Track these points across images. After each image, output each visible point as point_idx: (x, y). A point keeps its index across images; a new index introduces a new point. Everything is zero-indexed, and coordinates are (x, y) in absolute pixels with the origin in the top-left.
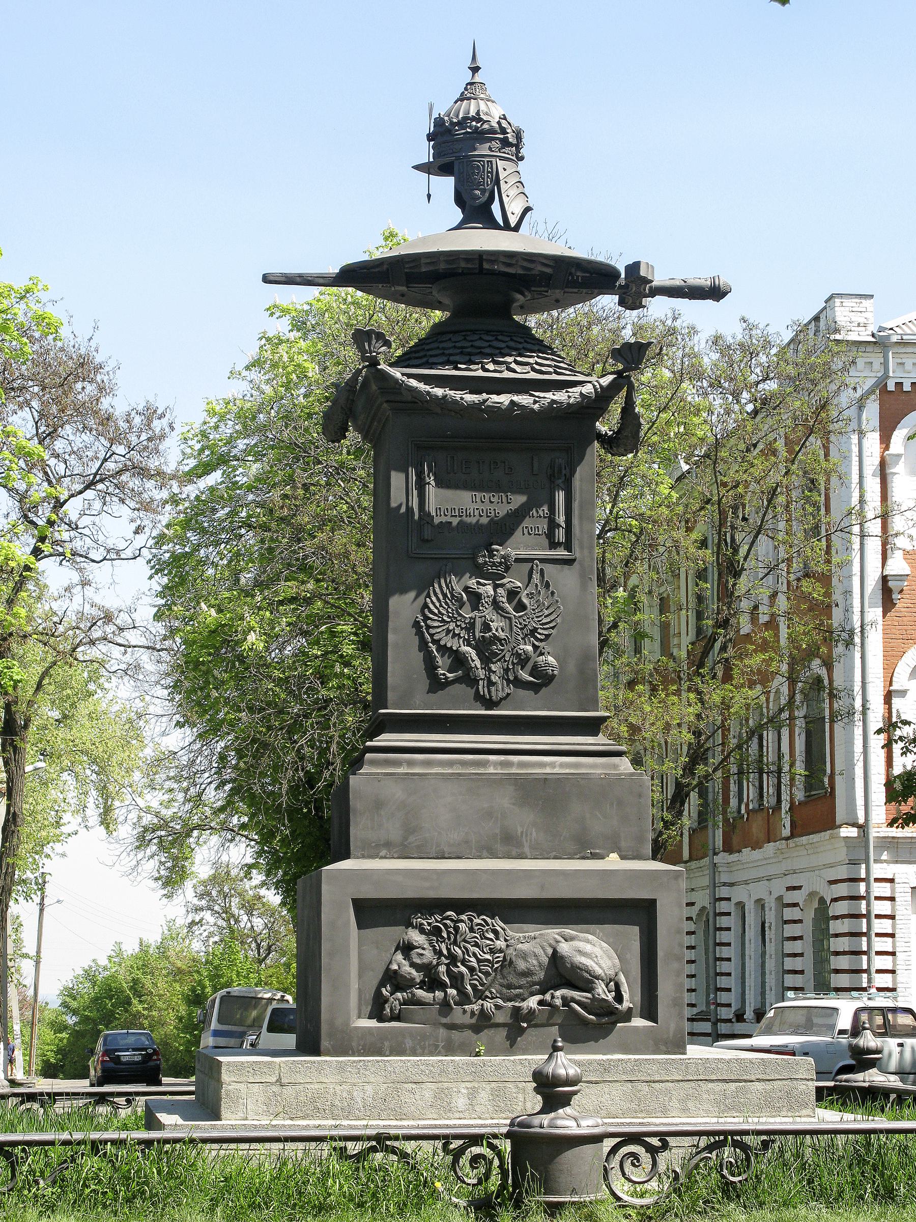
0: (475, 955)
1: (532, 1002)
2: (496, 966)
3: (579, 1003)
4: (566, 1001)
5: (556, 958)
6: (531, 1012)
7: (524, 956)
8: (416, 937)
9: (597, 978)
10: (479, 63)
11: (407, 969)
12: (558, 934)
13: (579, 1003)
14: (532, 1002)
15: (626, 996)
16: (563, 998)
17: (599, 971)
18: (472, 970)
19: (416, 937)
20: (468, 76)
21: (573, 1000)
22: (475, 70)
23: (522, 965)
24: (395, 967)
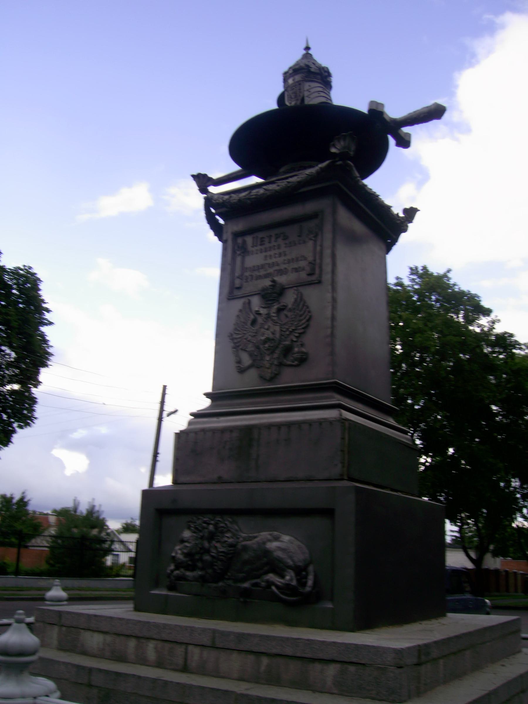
0: (216, 548)
1: (246, 585)
2: (230, 556)
3: (277, 587)
4: (270, 584)
5: (267, 553)
6: (246, 589)
7: (245, 548)
8: (187, 534)
9: (290, 567)
10: (311, 45)
11: (180, 556)
12: (270, 535)
13: (277, 587)
14: (246, 585)
15: (310, 582)
16: (268, 581)
17: (290, 563)
18: (213, 557)
19: (187, 534)
20: (304, 52)
21: (273, 584)
22: (307, 48)
23: (246, 556)
24: (173, 554)
